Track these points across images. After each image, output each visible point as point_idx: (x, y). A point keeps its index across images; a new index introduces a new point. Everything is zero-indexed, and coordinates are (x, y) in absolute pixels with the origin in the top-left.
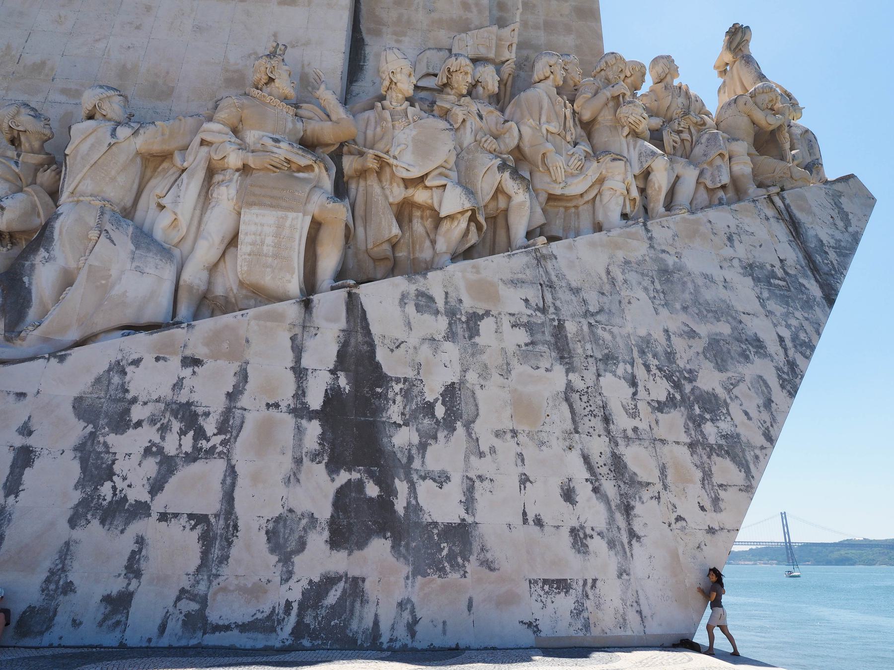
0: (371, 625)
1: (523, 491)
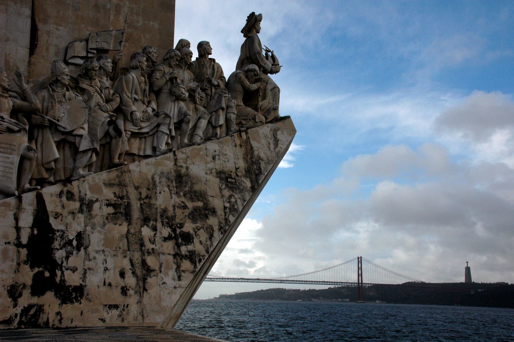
0: (46, 320)
1: (105, 274)
